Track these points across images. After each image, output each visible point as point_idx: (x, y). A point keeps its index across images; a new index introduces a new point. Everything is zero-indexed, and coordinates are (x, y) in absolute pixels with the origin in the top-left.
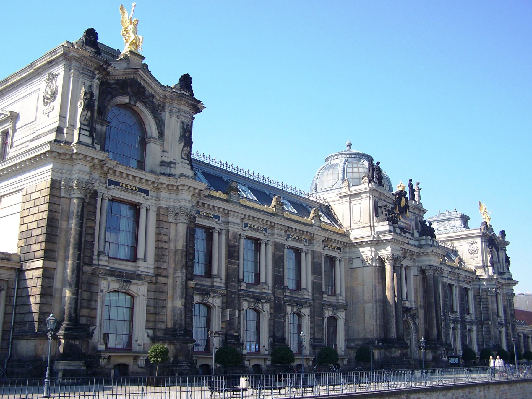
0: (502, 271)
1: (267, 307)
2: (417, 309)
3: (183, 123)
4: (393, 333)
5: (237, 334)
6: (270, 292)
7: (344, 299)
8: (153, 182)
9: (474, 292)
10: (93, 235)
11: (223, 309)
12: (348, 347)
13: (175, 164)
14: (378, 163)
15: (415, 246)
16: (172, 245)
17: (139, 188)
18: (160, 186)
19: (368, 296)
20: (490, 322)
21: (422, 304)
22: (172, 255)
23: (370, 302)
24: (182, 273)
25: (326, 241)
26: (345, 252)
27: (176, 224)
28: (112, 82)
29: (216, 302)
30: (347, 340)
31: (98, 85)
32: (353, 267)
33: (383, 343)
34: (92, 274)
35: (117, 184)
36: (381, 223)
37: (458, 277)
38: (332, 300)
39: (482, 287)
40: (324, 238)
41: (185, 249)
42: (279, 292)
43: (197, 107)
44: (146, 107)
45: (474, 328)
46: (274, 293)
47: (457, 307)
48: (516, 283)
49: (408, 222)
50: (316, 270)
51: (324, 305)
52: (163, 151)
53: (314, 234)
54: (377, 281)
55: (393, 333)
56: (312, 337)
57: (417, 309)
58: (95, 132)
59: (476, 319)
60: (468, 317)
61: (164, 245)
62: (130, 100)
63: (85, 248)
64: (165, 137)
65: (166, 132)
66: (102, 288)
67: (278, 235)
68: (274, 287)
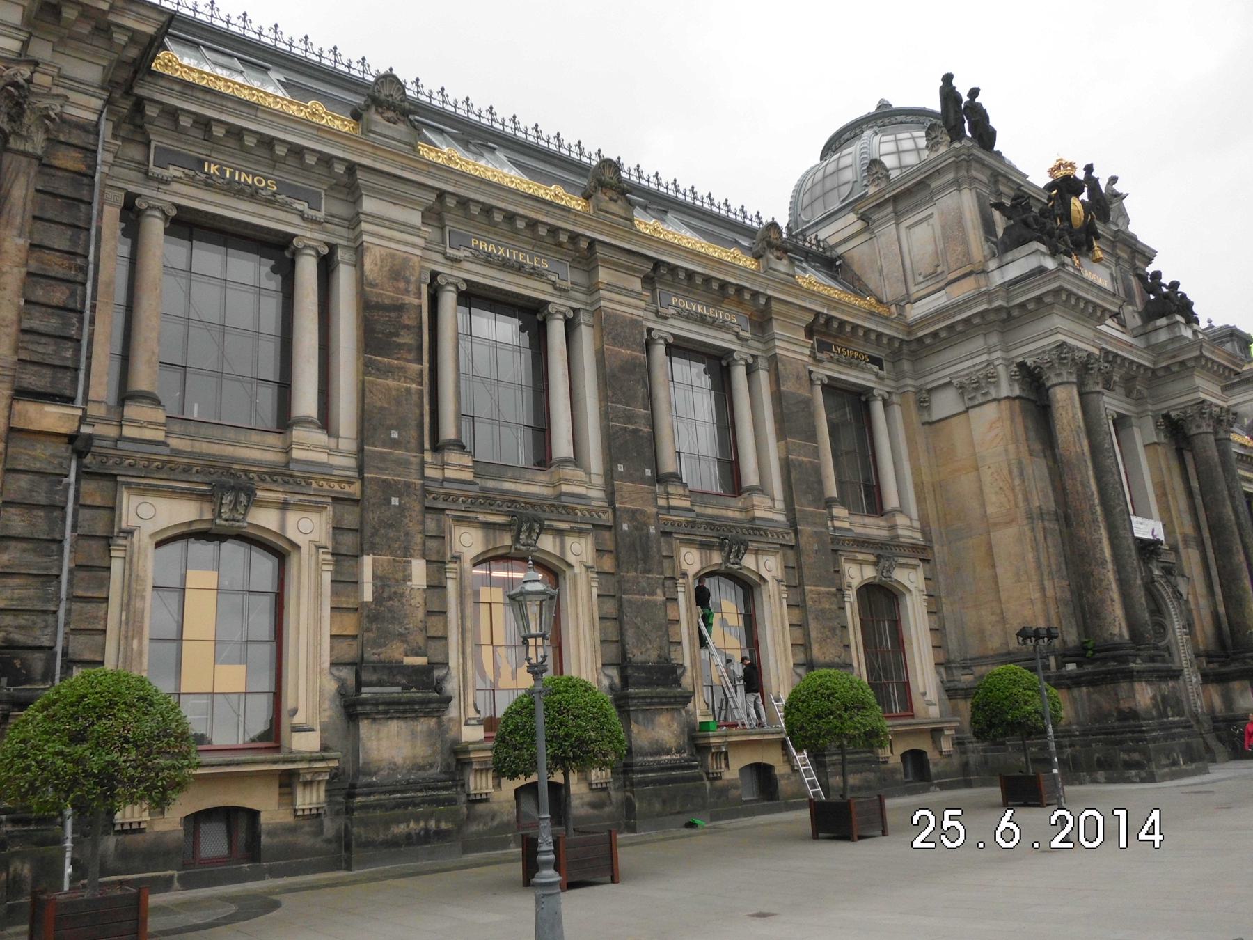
1: (579, 551)
4: (1117, 624)
5: (421, 661)
6: (597, 494)
7: (917, 524)
12: (951, 692)
14: (974, 93)
19: (995, 503)
21: (1189, 530)
23: (1009, 523)
25: (824, 332)
26: (899, 376)
29: (307, 529)
30: (944, 665)
32: (935, 418)
33: (1080, 665)
36: (1009, 256)
38: (873, 528)
42: (633, 496)
50: (791, 420)
53: (769, 298)
54: (1024, 449)
55: (1117, 624)
56: (801, 658)
68: (609, 474)
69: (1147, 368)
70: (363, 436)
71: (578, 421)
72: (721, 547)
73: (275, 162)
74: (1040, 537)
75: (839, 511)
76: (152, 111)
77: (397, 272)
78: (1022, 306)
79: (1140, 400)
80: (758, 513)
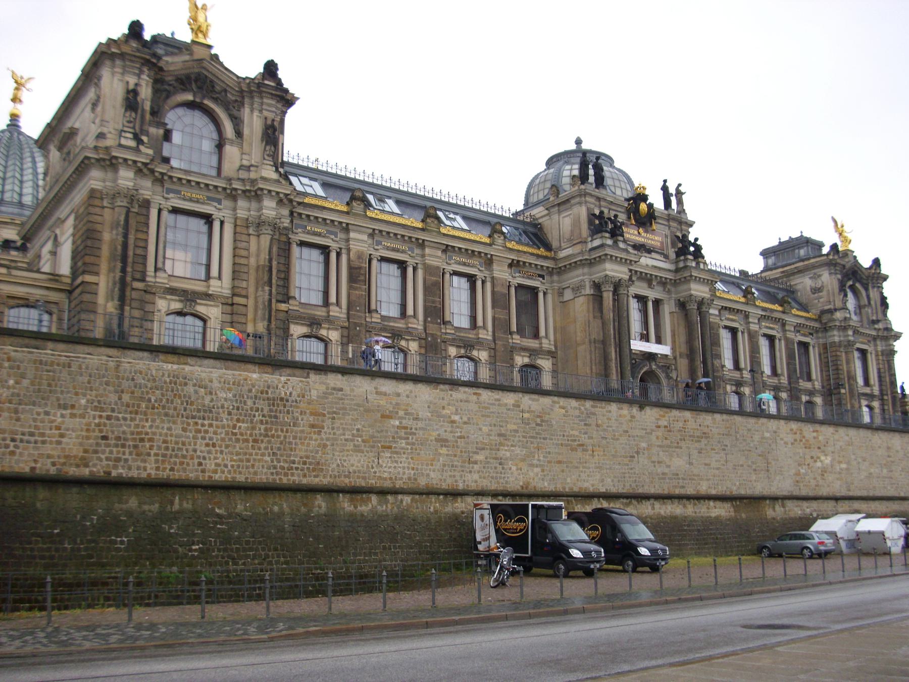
0: (874, 318)
1: (413, 346)
2: (675, 358)
3: (266, 118)
7: (552, 343)
8: (225, 189)
9: (819, 348)
10: (146, 248)
11: (344, 345)
13: (257, 167)
15: (669, 270)
16: (253, 261)
17: (207, 197)
18: (234, 193)
19: (580, 336)
20: (843, 391)
22: (252, 272)
23: (584, 343)
24: (263, 291)
26: (552, 282)
27: (258, 236)
28: (170, 78)
29: (334, 336)
31: (150, 84)
32: (565, 299)
34: (145, 291)
35: (179, 192)
37: (784, 325)
38: (533, 344)
39: (830, 340)
40: (510, 261)
41: (267, 263)
42: (433, 329)
43: (286, 100)
44: (217, 104)
45: (818, 400)
46: (425, 329)
47: (783, 367)
48: (897, 336)
49: (656, 238)
50: (500, 301)
51: (512, 350)
52: (242, 154)
53: (492, 255)
54: (591, 315)
57: (675, 358)
58: (148, 135)
59: (823, 387)
60: (804, 384)
61: (243, 261)
62: (194, 96)
63: (134, 262)
64: (245, 137)
65: (246, 131)
66: (160, 308)
67: (430, 255)
68: (425, 321)
69: (671, 280)
70: (349, 309)
71: (417, 303)
72: (464, 347)
73: (326, 224)
74: (593, 349)
75: (516, 336)
76: (295, 214)
77: (360, 256)
78: (595, 259)
79: (669, 292)
80: (480, 336)
